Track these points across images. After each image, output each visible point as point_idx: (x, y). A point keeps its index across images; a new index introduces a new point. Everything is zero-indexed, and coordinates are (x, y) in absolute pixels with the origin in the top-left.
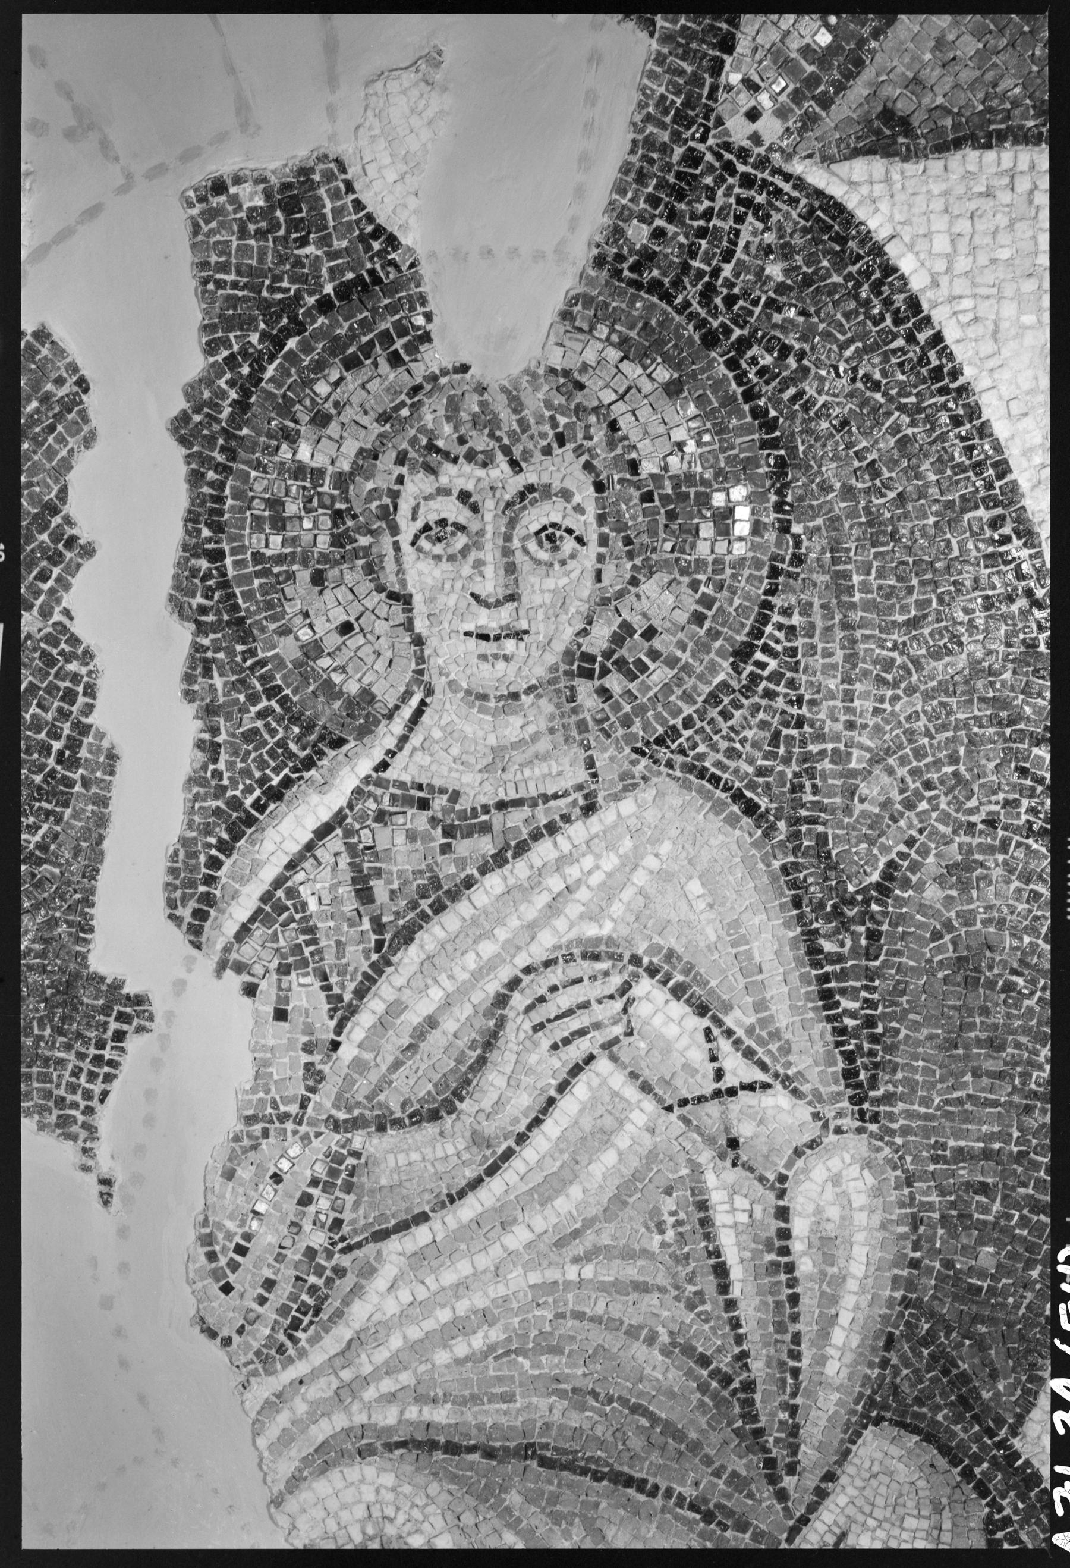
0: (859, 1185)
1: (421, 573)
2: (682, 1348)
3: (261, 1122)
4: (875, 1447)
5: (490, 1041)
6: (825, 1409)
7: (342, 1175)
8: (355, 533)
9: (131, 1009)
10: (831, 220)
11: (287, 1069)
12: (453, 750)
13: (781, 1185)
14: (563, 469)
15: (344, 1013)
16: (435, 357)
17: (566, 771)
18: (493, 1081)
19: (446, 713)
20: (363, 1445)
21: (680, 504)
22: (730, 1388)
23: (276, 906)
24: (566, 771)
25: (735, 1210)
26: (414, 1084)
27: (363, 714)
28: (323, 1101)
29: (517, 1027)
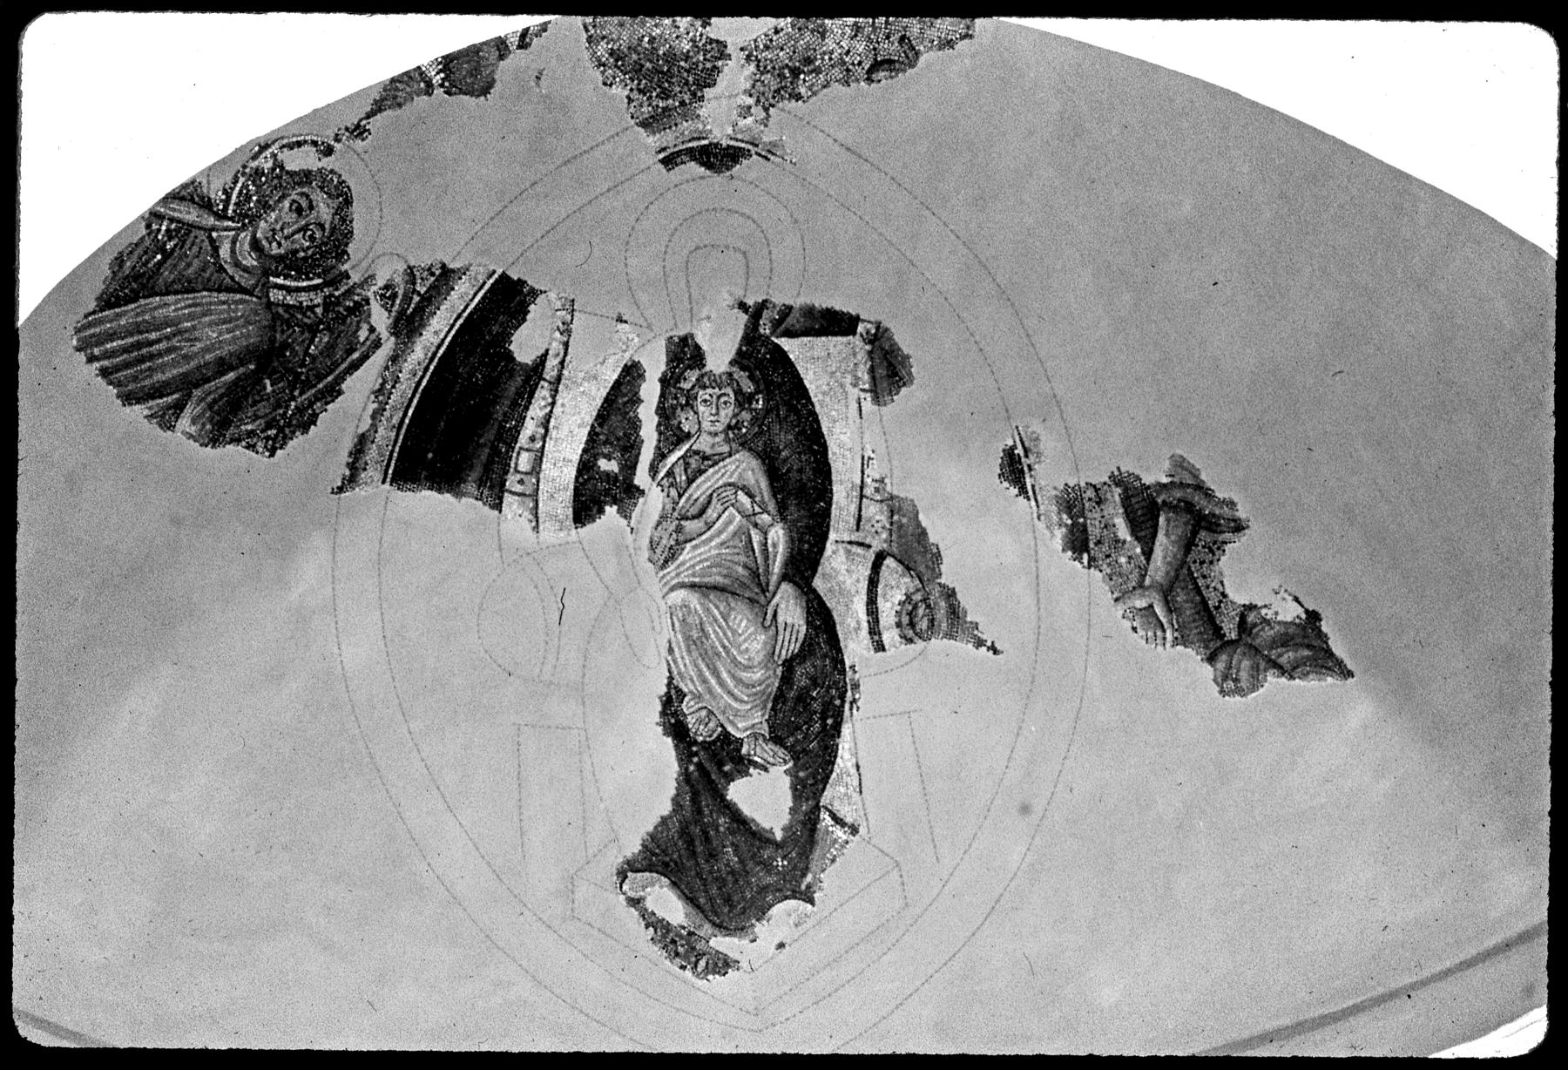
0: (781, 532)
1: (701, 409)
2: (745, 567)
3: (663, 517)
4: (784, 586)
5: (709, 502)
6: (774, 579)
7: (679, 530)
8: (690, 399)
9: (642, 492)
10: (778, 348)
11: (669, 507)
12: (704, 444)
13: (766, 533)
14: (729, 390)
15: (680, 496)
16: (707, 369)
17: (726, 449)
18: (709, 511)
19: (704, 437)
20: (682, 586)
21: (750, 398)
22: (755, 574)
23: (670, 473)
24: (726, 449)
25: (756, 538)
26: (694, 511)
27: (688, 436)
28: (676, 514)
29: (714, 500)
